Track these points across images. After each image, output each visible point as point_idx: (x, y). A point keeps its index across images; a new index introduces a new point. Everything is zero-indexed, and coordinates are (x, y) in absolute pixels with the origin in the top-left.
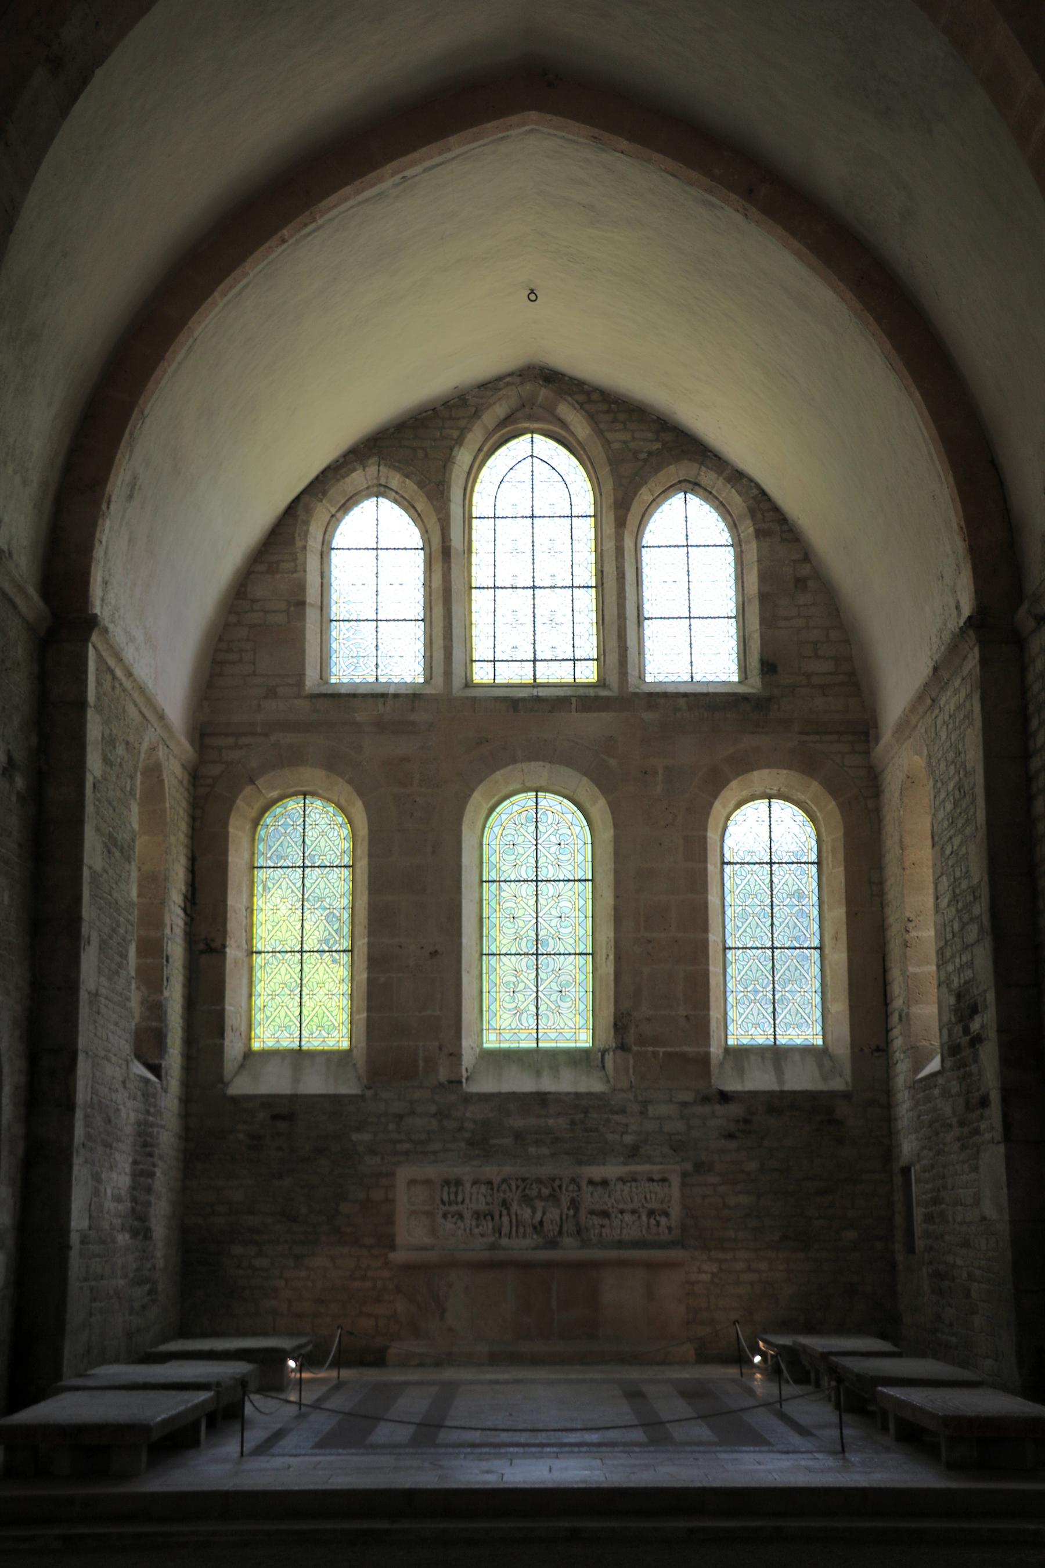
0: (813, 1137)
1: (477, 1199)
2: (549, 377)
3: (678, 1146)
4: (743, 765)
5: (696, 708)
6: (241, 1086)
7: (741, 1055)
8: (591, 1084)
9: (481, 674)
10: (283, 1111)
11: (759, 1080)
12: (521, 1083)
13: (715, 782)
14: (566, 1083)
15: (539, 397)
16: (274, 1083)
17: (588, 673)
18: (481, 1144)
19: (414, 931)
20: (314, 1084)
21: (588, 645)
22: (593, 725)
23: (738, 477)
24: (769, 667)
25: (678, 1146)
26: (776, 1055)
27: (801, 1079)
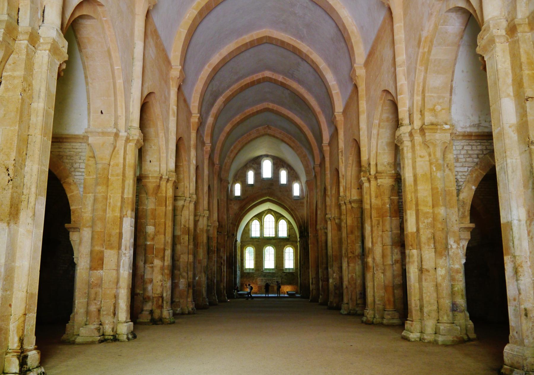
0: (289, 277)
1: (264, 281)
2: (271, 210)
3: (281, 276)
4: (287, 245)
5: (283, 239)
6: (245, 271)
7: (286, 269)
8: (274, 271)
9: (265, 236)
10: (249, 273)
11: (288, 271)
12: (268, 271)
13: (284, 246)
14: (272, 271)
15: (270, 211)
16: (248, 271)
17: (274, 236)
18: (265, 276)
19: (259, 258)
20: (251, 271)
21: (274, 233)
22: (274, 241)
23: (287, 219)
24: (289, 236)
25: (281, 276)
26: (289, 269)
27: (291, 271)
